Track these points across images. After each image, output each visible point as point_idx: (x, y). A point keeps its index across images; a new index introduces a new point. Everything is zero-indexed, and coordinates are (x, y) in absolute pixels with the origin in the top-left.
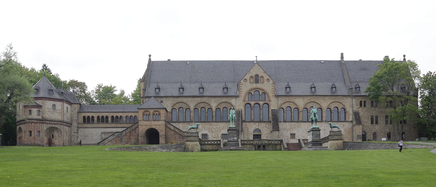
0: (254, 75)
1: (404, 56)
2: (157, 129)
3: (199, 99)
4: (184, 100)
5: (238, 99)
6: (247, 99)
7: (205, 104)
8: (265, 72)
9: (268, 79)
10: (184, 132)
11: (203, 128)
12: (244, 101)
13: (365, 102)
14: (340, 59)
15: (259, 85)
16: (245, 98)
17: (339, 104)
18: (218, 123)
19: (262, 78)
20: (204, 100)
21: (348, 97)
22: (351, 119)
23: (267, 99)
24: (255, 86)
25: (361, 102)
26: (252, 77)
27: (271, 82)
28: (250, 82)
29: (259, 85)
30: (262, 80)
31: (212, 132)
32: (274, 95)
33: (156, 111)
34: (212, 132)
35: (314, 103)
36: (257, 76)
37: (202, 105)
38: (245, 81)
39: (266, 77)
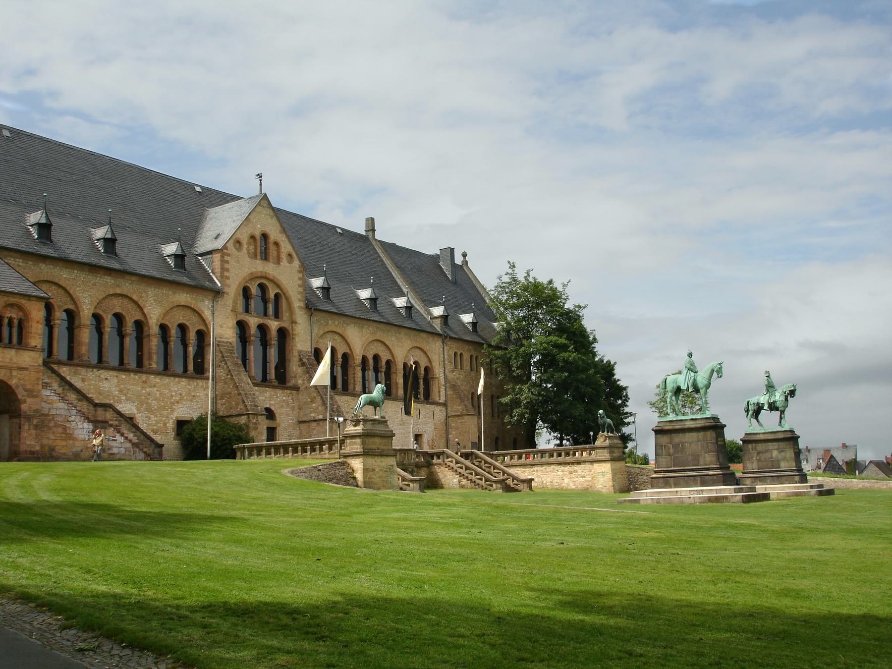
0: (258, 234)
1: (464, 255)
2: (13, 382)
3: (109, 280)
4: (63, 275)
5: (221, 302)
6: (240, 307)
7: (126, 301)
8: (284, 231)
9: (290, 255)
10: (96, 405)
11: (121, 391)
12: (234, 310)
13: (461, 354)
14: (364, 233)
15: (269, 269)
16: (235, 302)
17: (422, 354)
18: (167, 380)
19: (275, 248)
20: (127, 287)
21: (436, 338)
22: (442, 400)
23: (285, 315)
24: (260, 266)
25: (455, 354)
26: (253, 237)
27: (296, 263)
28: (248, 253)
29: (269, 269)
30: (275, 253)
31: (149, 410)
32: (302, 304)
33: (12, 305)
34: (149, 410)
35: (379, 344)
36: (265, 236)
37: (118, 306)
38: (238, 245)
39: (286, 248)
